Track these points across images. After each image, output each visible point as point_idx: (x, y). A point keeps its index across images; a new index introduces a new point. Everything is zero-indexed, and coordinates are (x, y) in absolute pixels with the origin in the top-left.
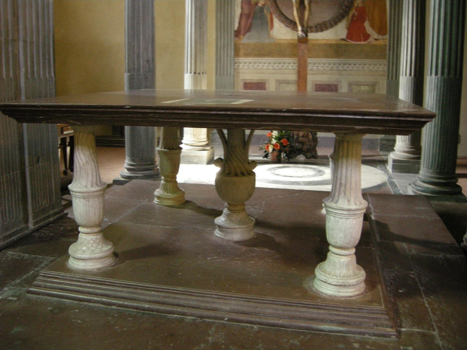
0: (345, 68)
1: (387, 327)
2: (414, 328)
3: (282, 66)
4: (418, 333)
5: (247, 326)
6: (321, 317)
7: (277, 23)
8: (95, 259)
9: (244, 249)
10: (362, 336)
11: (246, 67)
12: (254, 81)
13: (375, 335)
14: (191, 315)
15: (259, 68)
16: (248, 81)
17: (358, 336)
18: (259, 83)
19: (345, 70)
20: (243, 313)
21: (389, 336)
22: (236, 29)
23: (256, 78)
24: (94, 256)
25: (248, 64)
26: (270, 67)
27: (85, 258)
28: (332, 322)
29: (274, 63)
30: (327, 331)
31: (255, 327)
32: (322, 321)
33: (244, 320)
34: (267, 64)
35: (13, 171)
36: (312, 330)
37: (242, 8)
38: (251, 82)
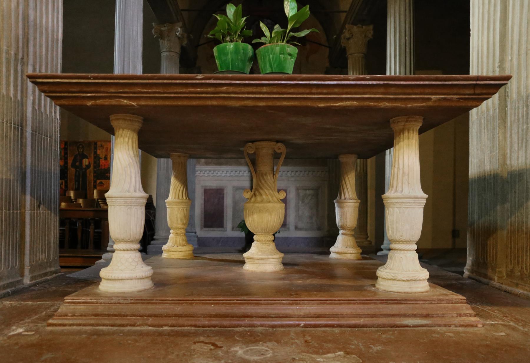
0: (293, 175)
1: (470, 316)
3: (238, 174)
6: (403, 312)
11: (206, 175)
12: (213, 188)
13: (461, 326)
14: (262, 326)
15: (218, 175)
16: (208, 188)
18: (218, 190)
19: (292, 177)
20: (319, 316)
21: (476, 325)
23: (215, 185)
24: (134, 276)
25: (208, 172)
26: (228, 175)
28: (414, 316)
30: (411, 326)
32: (405, 316)
34: (225, 172)
35: (13, 210)
38: (211, 188)
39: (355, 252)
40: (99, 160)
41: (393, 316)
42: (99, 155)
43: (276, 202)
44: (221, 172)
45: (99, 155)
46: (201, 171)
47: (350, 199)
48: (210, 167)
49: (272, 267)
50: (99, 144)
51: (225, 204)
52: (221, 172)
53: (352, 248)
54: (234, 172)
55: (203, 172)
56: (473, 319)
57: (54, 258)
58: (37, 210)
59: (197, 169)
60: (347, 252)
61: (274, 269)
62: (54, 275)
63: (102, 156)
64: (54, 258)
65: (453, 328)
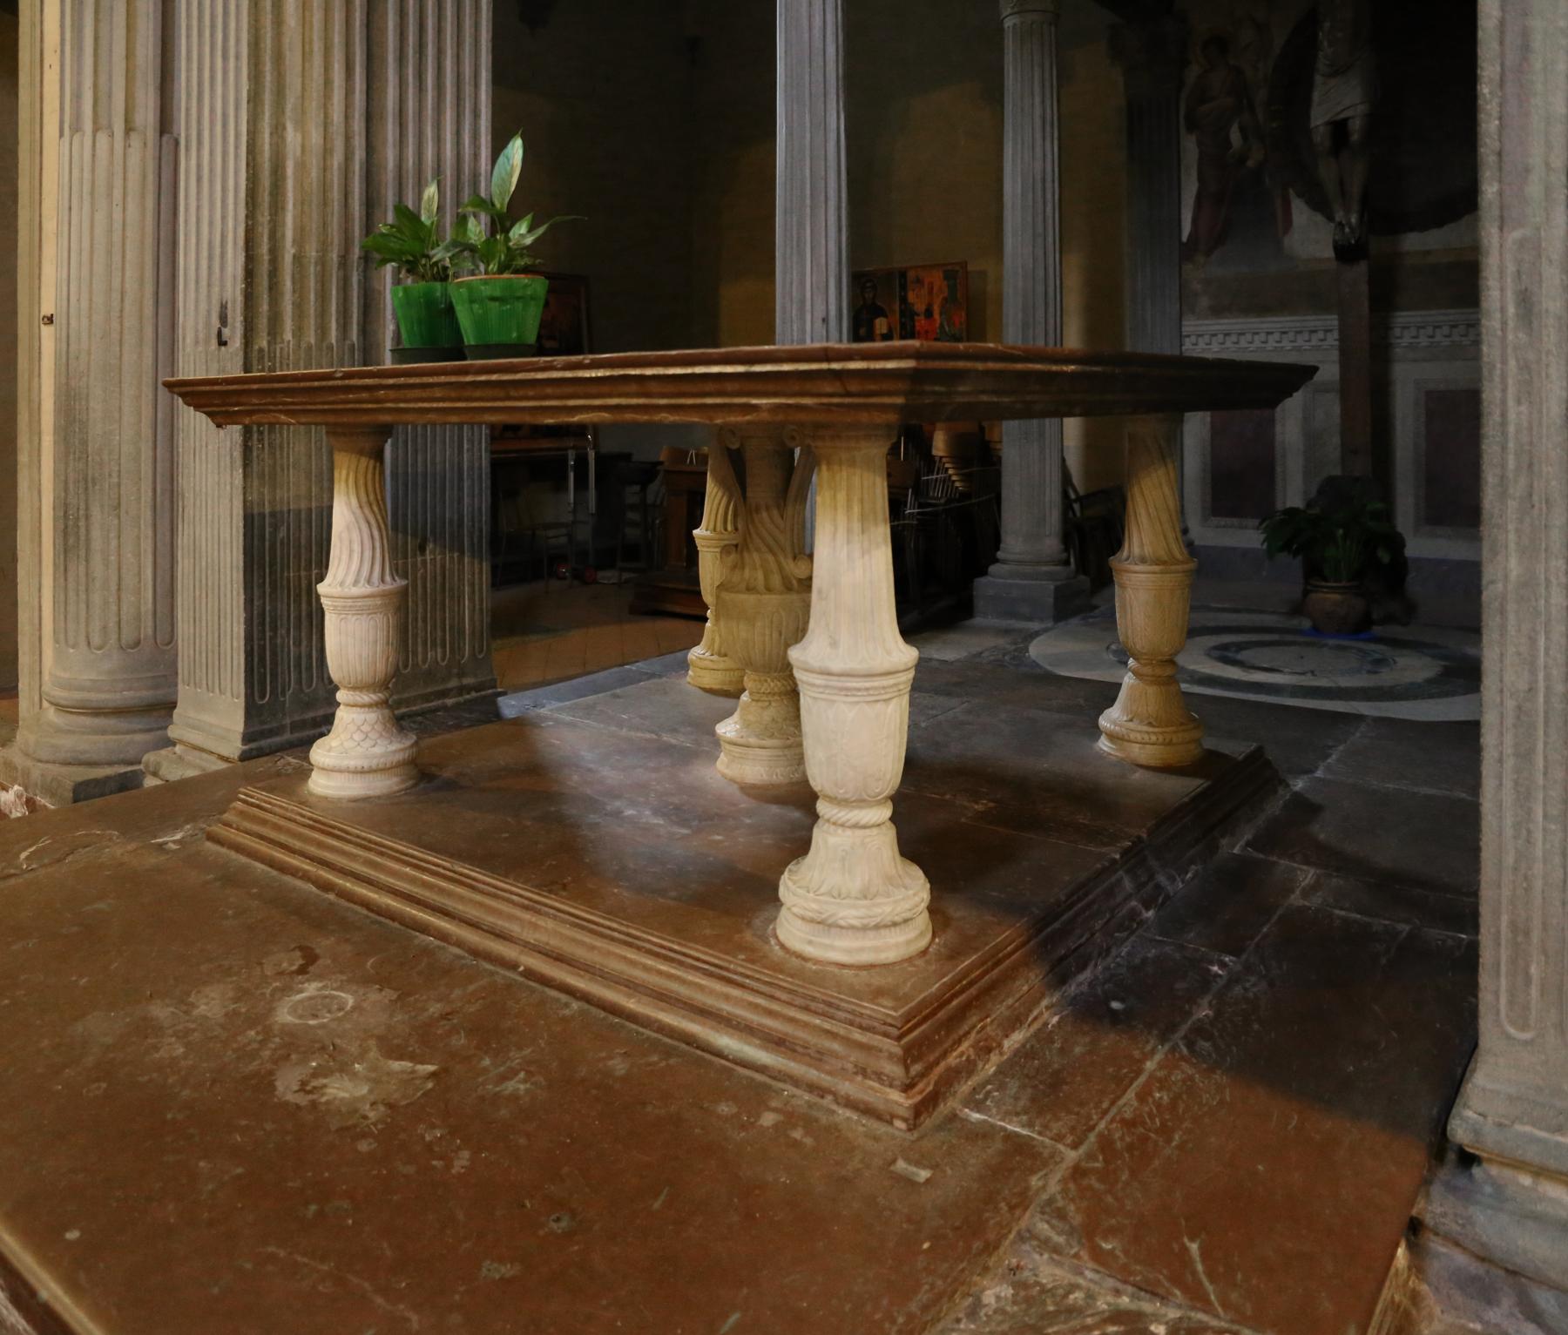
1: (891, 1086)
2: (1015, 1119)
3: (1322, 340)
4: (1010, 1137)
5: (558, 1000)
7: (1301, 213)
8: (348, 771)
9: (743, 806)
10: (814, 1099)
15: (1252, 347)
17: (807, 1097)
20: (559, 958)
21: (888, 1117)
22: (1184, 239)
24: (345, 763)
26: (1287, 344)
27: (326, 766)
29: (1297, 332)
30: (731, 1057)
31: (576, 1005)
33: (554, 980)
34: (1276, 336)
36: (697, 1048)
37: (1201, 179)
39: (1154, 738)
40: (913, 320)
41: (703, 1013)
42: (913, 304)
43: (769, 590)
44: (1263, 337)
45: (913, 304)
46: (1199, 336)
47: (1143, 560)
48: (1226, 321)
49: (762, 770)
50: (911, 275)
51: (1278, 438)
52: (1263, 337)
53: (1150, 724)
54: (1306, 336)
55: (1207, 338)
56: (896, 1096)
57: (474, 655)
58: (414, 556)
59: (1186, 330)
60: (1126, 737)
61: (765, 777)
62: (474, 694)
63: (920, 307)
64: (473, 655)
65: (828, 1101)
